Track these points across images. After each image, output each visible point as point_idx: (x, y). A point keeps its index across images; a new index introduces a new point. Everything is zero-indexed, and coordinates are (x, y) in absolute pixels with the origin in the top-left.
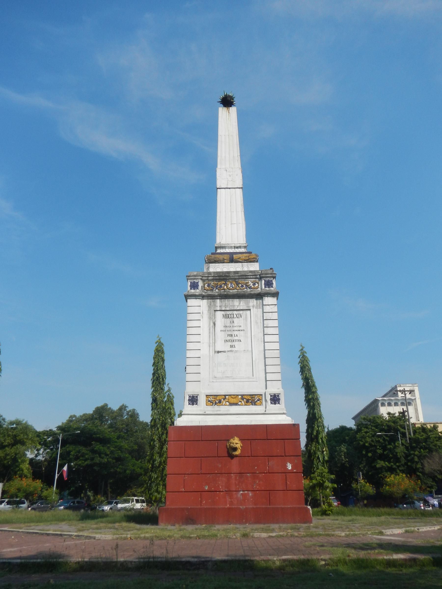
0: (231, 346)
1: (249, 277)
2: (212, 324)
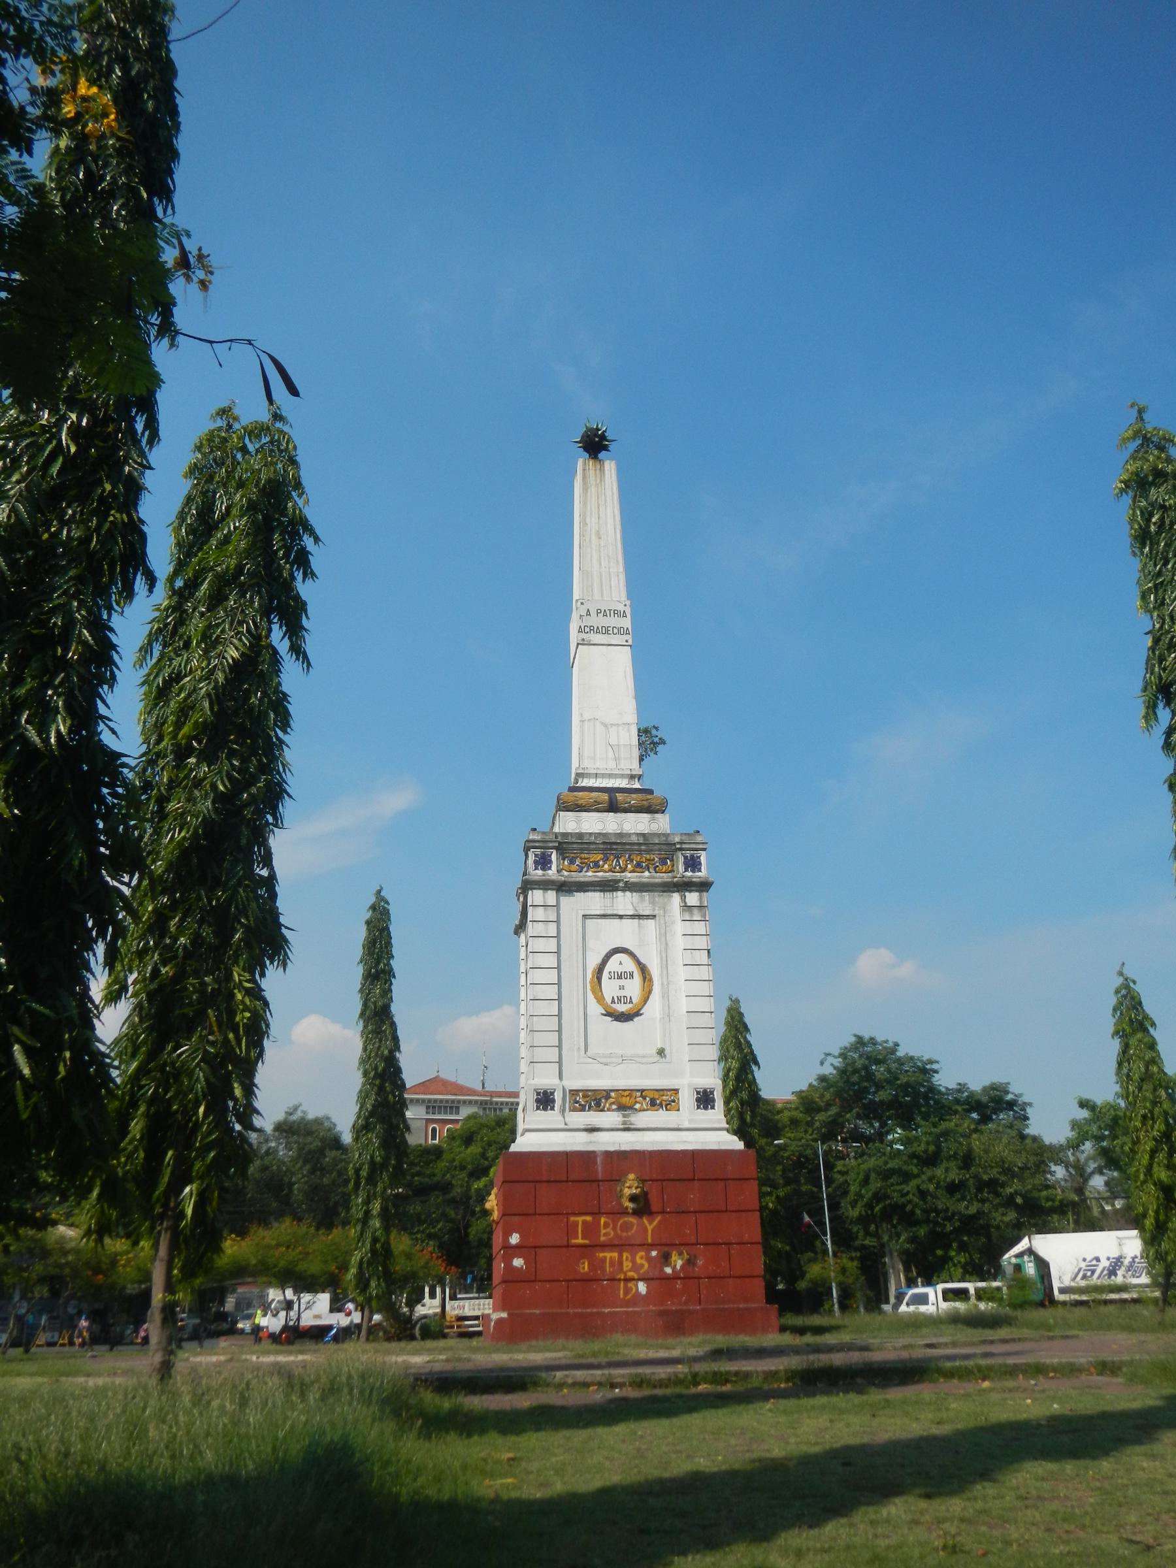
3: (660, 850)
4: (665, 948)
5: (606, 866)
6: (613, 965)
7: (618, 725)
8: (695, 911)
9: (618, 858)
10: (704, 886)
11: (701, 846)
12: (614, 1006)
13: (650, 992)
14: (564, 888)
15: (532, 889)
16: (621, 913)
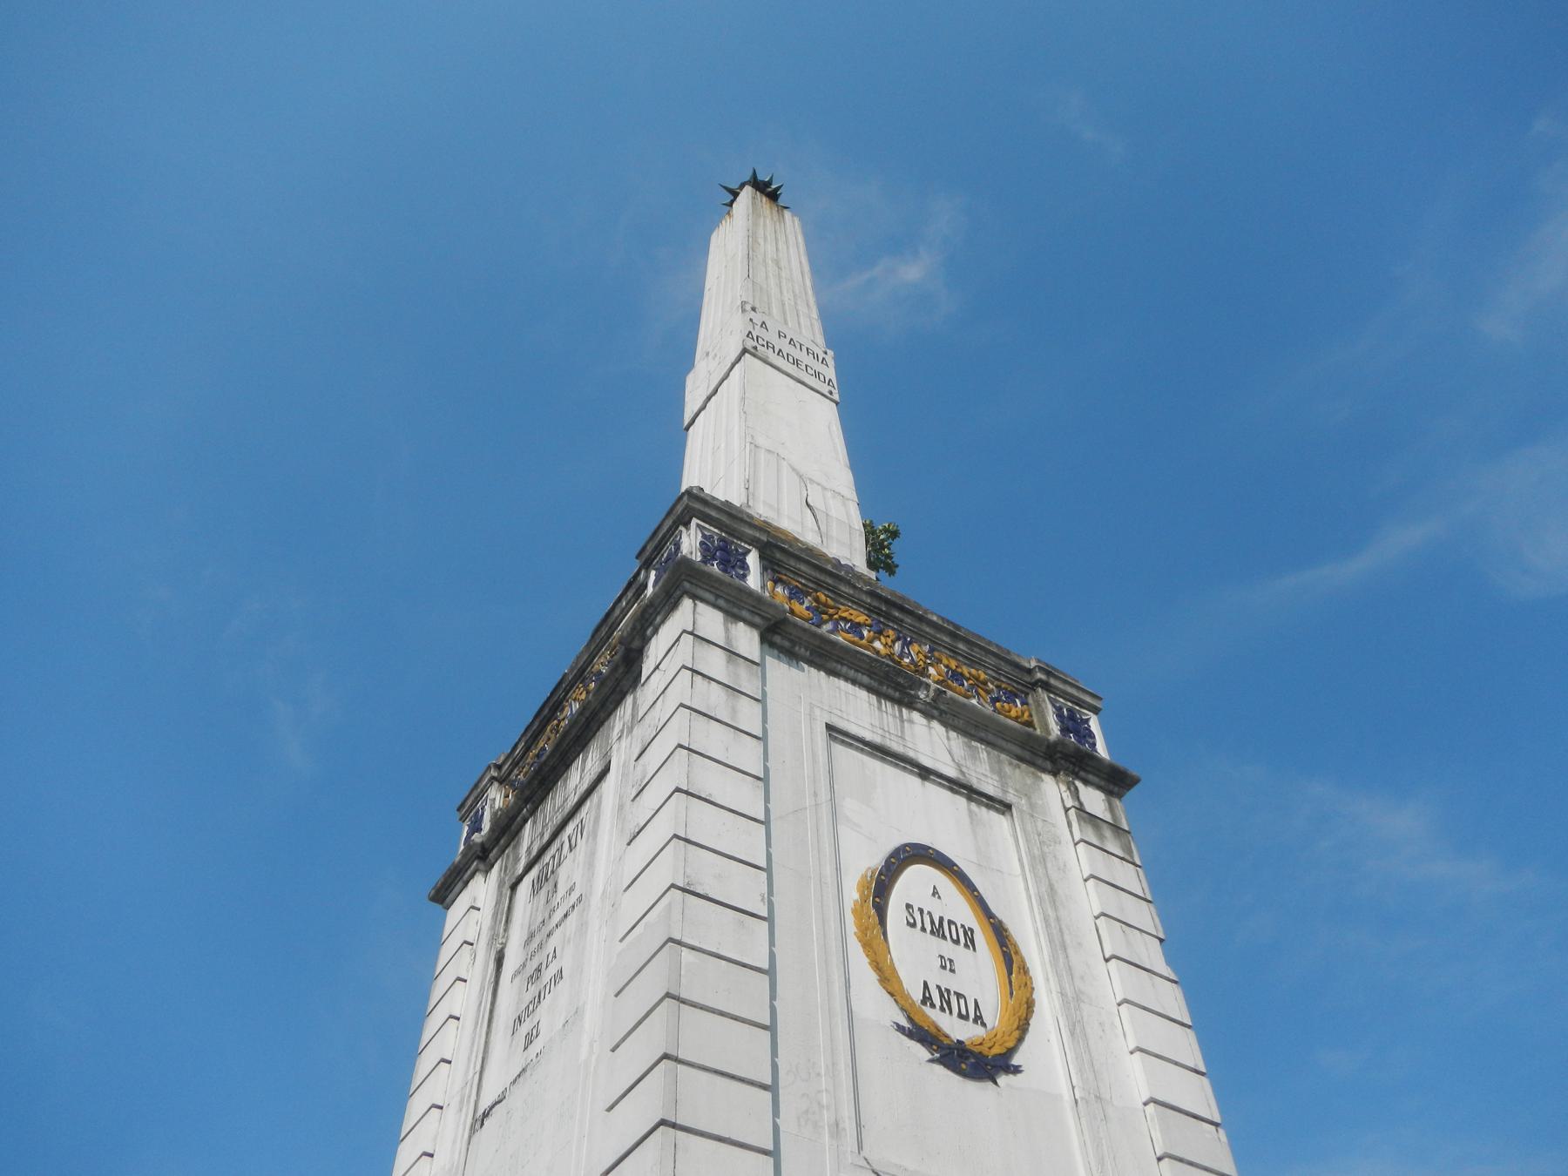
0: (529, 1040)
1: (617, 612)
2: (492, 966)
3: (997, 670)
4: (1050, 898)
7: (824, 489)
8: (1108, 833)
9: (907, 644)
10: (1115, 781)
11: (1088, 699)
12: (927, 1009)
13: (1030, 1005)
15: (694, 597)
16: (927, 762)
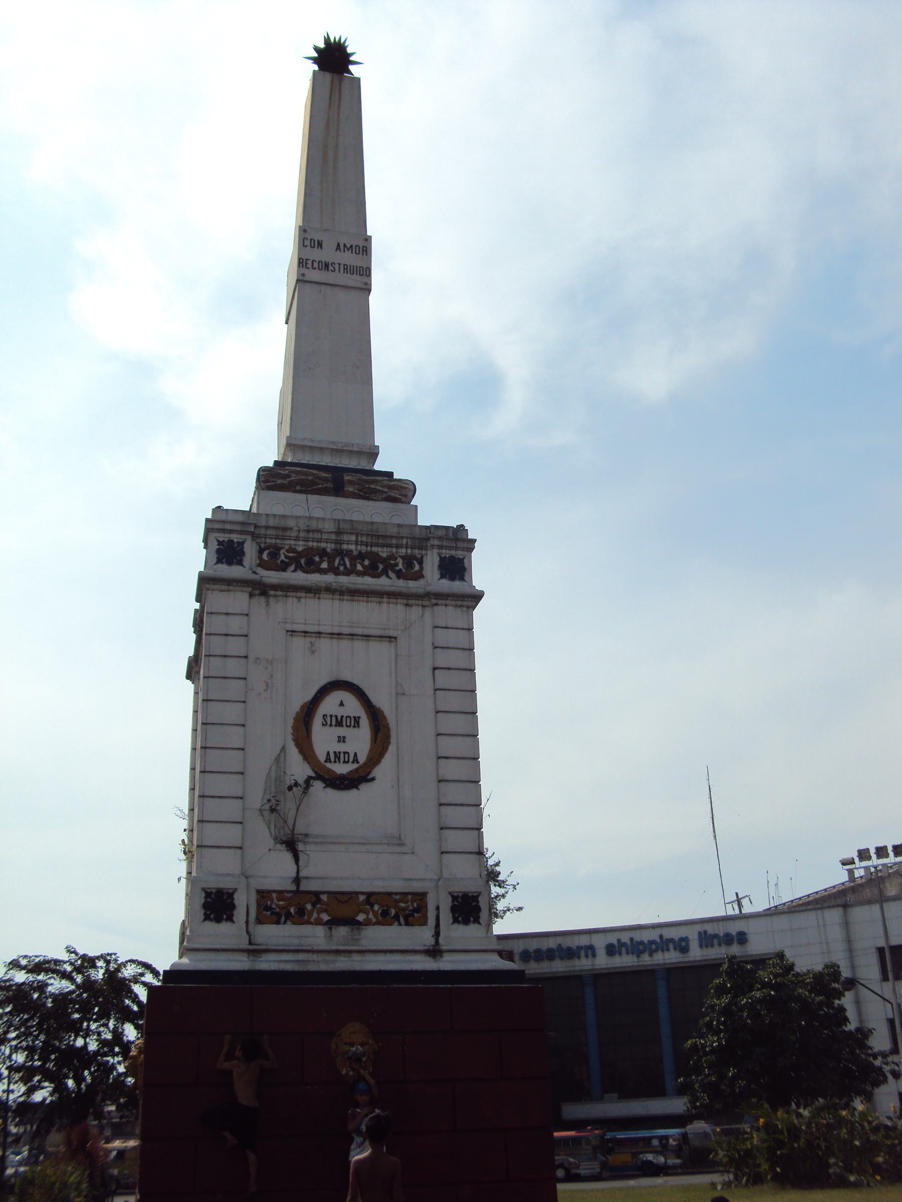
5: (324, 565)
6: (329, 705)
12: (328, 765)
14: (260, 590)
